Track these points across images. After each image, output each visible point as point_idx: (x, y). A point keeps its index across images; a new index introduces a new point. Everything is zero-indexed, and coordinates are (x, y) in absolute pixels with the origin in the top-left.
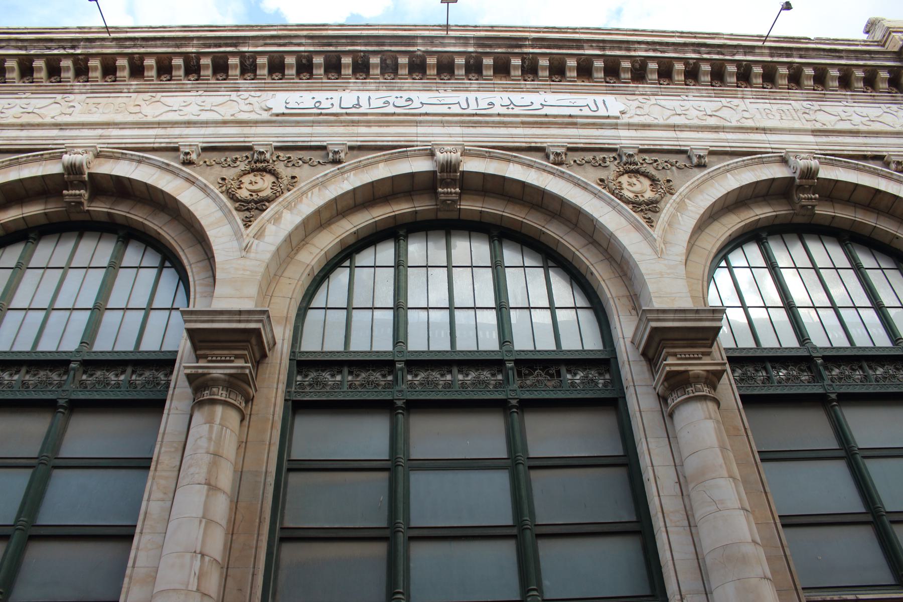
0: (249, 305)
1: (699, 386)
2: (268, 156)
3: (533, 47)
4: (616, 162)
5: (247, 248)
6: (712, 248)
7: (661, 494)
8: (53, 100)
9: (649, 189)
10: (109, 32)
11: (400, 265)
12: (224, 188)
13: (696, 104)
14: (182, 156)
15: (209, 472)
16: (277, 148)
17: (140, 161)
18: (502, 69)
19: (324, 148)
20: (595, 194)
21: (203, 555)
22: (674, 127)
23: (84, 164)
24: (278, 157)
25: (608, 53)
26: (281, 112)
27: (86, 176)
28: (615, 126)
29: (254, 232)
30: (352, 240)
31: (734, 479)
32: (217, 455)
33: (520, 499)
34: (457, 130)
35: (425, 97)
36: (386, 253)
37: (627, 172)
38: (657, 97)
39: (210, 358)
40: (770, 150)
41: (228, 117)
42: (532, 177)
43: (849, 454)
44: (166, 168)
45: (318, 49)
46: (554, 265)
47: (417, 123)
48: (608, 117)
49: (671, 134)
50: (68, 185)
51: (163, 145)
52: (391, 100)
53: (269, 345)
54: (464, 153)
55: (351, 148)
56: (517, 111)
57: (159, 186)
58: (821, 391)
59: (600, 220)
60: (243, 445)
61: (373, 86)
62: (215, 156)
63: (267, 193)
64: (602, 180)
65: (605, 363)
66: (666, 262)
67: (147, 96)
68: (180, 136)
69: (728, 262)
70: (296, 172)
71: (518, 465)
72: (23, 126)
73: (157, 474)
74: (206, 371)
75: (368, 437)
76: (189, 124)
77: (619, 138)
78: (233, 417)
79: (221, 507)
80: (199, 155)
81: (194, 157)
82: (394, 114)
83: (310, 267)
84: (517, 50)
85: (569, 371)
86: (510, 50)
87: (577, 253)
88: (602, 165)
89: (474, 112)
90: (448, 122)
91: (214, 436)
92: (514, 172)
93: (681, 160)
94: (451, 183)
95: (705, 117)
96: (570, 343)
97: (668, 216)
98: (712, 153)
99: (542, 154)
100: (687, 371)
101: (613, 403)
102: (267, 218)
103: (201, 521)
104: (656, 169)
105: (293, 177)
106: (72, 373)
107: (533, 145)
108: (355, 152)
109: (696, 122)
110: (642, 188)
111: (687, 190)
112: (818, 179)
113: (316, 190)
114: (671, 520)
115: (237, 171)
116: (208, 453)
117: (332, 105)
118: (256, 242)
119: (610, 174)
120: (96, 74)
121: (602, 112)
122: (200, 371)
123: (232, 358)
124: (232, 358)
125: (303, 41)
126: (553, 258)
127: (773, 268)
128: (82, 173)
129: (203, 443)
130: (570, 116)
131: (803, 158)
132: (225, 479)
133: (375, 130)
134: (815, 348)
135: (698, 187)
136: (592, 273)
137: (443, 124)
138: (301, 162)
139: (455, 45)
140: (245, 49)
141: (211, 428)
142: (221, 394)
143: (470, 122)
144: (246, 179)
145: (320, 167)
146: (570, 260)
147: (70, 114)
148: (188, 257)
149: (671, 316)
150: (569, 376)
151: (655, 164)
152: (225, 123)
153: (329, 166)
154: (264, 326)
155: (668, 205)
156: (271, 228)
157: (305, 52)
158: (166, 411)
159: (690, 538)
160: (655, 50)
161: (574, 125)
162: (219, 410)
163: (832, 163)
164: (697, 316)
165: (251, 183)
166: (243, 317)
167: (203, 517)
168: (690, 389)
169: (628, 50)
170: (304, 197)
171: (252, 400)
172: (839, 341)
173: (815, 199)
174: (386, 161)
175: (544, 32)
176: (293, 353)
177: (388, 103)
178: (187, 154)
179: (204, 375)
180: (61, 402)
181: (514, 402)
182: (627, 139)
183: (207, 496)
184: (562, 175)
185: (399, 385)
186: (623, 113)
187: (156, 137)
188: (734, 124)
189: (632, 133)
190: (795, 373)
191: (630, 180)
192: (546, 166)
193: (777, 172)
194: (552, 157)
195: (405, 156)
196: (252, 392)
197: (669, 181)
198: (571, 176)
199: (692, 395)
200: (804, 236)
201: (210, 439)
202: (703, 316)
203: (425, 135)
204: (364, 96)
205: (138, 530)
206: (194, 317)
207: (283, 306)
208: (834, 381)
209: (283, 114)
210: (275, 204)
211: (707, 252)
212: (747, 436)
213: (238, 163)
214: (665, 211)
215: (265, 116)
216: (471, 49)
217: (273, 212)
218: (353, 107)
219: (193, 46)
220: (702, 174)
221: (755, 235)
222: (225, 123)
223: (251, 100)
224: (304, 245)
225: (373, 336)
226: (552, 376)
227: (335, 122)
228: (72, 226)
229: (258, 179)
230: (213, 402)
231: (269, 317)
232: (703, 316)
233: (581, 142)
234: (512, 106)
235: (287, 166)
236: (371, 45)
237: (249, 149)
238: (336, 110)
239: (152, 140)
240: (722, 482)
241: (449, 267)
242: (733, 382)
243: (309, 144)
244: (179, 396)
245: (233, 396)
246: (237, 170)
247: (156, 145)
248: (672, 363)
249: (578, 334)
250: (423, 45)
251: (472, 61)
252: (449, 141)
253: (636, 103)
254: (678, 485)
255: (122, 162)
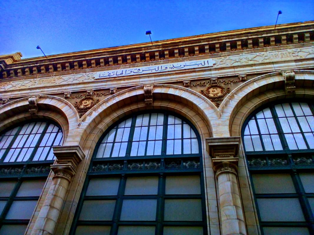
0: (76, 144)
1: (226, 168)
2: (91, 93)
3: (182, 45)
4: (209, 84)
5: (79, 125)
6: (246, 113)
7: (209, 211)
8: (30, 81)
9: (220, 92)
10: (47, 57)
11: (133, 127)
12: (76, 105)
13: (245, 57)
14: (65, 96)
15: (52, 202)
16: (94, 91)
17: (53, 98)
18: (172, 54)
19: (109, 89)
20: (199, 97)
21: (43, 231)
22: (234, 67)
23: (35, 101)
24: (94, 94)
25: (210, 42)
26: (97, 78)
27: (36, 105)
28: (210, 70)
29: (82, 119)
30: (117, 119)
31: (236, 206)
32: (55, 196)
33: (161, 210)
34: (153, 78)
35: (144, 68)
36: (129, 124)
37: (212, 87)
38: (229, 56)
39: (60, 163)
40: (274, 71)
41: (81, 82)
42: (177, 93)
43: (300, 195)
44: (59, 100)
45: (110, 56)
46: (185, 123)
47: (140, 78)
48: (208, 67)
49: (233, 70)
50: (31, 108)
51: (60, 93)
52: (133, 71)
53: (82, 157)
54: (155, 87)
55: (118, 88)
56: (175, 69)
57: (57, 106)
58: (289, 168)
59: (199, 106)
60: (68, 192)
61: (128, 66)
62: (75, 95)
63: (89, 106)
64: (202, 91)
65: (197, 158)
66: (222, 120)
67: (57, 77)
68: (65, 89)
69: (255, 117)
70: (100, 98)
71: (162, 198)
72: (20, 90)
73: (40, 202)
74: (57, 167)
75: (110, 187)
76: (68, 85)
77: (211, 74)
78: (65, 183)
79: (55, 214)
80: (71, 95)
81: (69, 96)
82: (133, 75)
83: (101, 130)
84: (176, 47)
85: (184, 162)
86: (174, 47)
87: (192, 118)
88: (203, 85)
89: (160, 71)
90: (150, 76)
91: (55, 189)
92: (171, 91)
93: (236, 80)
94: (150, 97)
95: (248, 61)
96: (187, 152)
97: (225, 102)
98: (248, 75)
99: (181, 84)
100: (222, 162)
101: (199, 174)
102: (87, 114)
103: (45, 219)
104: (225, 84)
105: (98, 100)
106: (24, 169)
107: (179, 81)
108: (119, 90)
109: (244, 64)
110: (216, 92)
111: (236, 91)
112: (296, 80)
113: (104, 104)
114: (212, 222)
115: (80, 99)
116: (52, 195)
117: (114, 74)
118: (83, 122)
119: (204, 89)
120: (13, 75)
121: (206, 65)
122: (55, 167)
123: (67, 162)
124: (67, 162)
125: (106, 54)
126: (185, 120)
127: (275, 118)
128: (35, 104)
129: (52, 192)
130: (194, 69)
131: (288, 73)
132: (58, 204)
133: (126, 81)
134: (289, 150)
135: (241, 89)
136: (196, 125)
137: (149, 77)
138: (101, 95)
139: (155, 48)
140: (88, 58)
141: (55, 186)
142: (61, 175)
143: (157, 75)
144: (83, 102)
145: (107, 96)
146: (190, 121)
147: (34, 85)
148: (64, 128)
149: (217, 141)
150: (184, 164)
151: (224, 83)
152: (79, 84)
153: (110, 95)
154: (78, 151)
155: (226, 98)
156: (88, 118)
157: (106, 57)
158: (47, 181)
159: (219, 230)
160: (229, 38)
161: (195, 72)
162: (59, 180)
163: (303, 73)
164: (228, 140)
165: (85, 103)
166: (71, 148)
167: (46, 217)
168: (223, 169)
169: (219, 40)
170: (100, 107)
171: (74, 176)
172: (302, 146)
173: (294, 88)
174: (129, 91)
175: (192, 38)
176: (92, 159)
177: (132, 71)
178: (66, 95)
179: (56, 168)
180: (19, 178)
181: (162, 174)
182: (214, 74)
183: (49, 210)
184: (187, 91)
185: (127, 168)
186: (214, 64)
187: (58, 90)
188: (260, 62)
189: (217, 72)
190: (279, 161)
191: (213, 90)
192: (182, 88)
193: (277, 79)
194: (185, 84)
195: (135, 89)
196: (74, 173)
197: (228, 88)
198: (190, 91)
199: (223, 171)
200: (292, 104)
201: (54, 190)
202: (230, 140)
203: (142, 81)
204: (124, 70)
205: (30, 221)
206: (56, 149)
207: (92, 142)
208: (297, 164)
209: (98, 79)
210: (90, 109)
211: (243, 114)
212: (250, 188)
213: (82, 97)
214: (224, 100)
215: (93, 80)
216: (160, 49)
217: (89, 112)
218: (120, 74)
219: (72, 59)
220: (243, 84)
221: (270, 105)
222: (79, 84)
223: (90, 75)
224: (100, 122)
225: (120, 152)
226: (178, 164)
227: (114, 80)
228: (33, 120)
229: (87, 101)
230: (58, 177)
231: (80, 148)
232: (230, 140)
233: (196, 78)
234: (173, 68)
235: (97, 96)
236: (127, 52)
237: (86, 92)
238: (115, 76)
239: (56, 91)
240: (230, 207)
241: (149, 126)
242: (246, 165)
243: (104, 88)
244: (52, 174)
245: (65, 175)
246: (81, 99)
247: (58, 93)
248: (217, 159)
249: (191, 148)
250: (144, 50)
251: (161, 53)
252: (148, 83)
253: (221, 60)
254: (217, 208)
255: (47, 99)
